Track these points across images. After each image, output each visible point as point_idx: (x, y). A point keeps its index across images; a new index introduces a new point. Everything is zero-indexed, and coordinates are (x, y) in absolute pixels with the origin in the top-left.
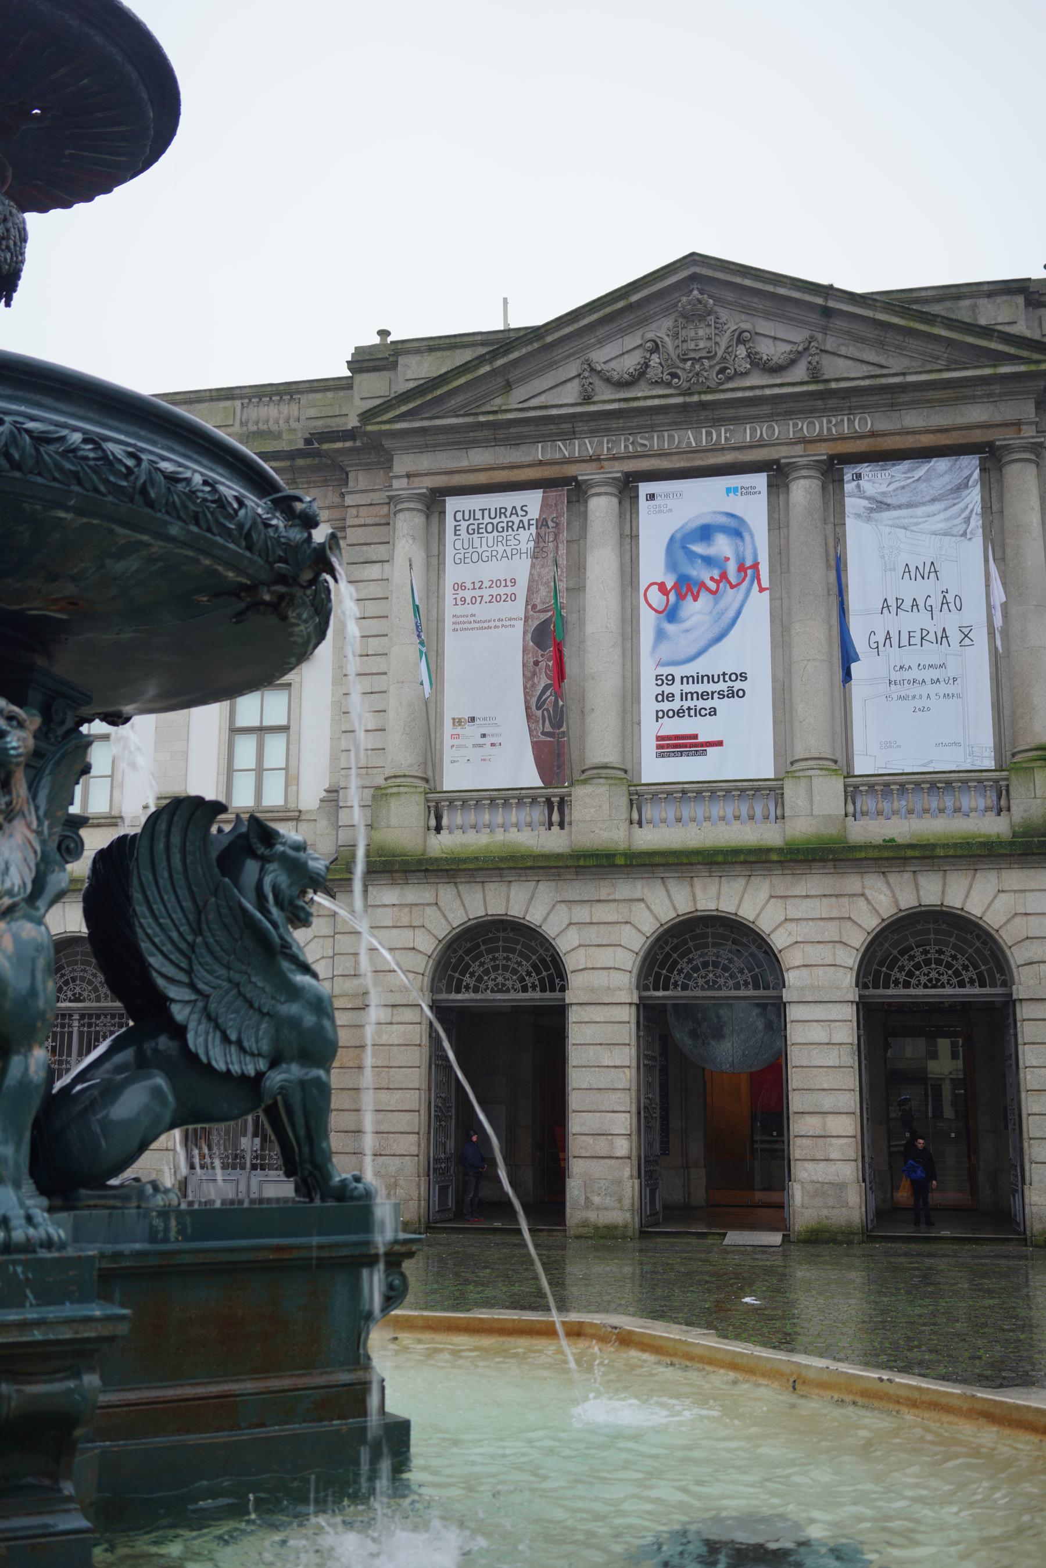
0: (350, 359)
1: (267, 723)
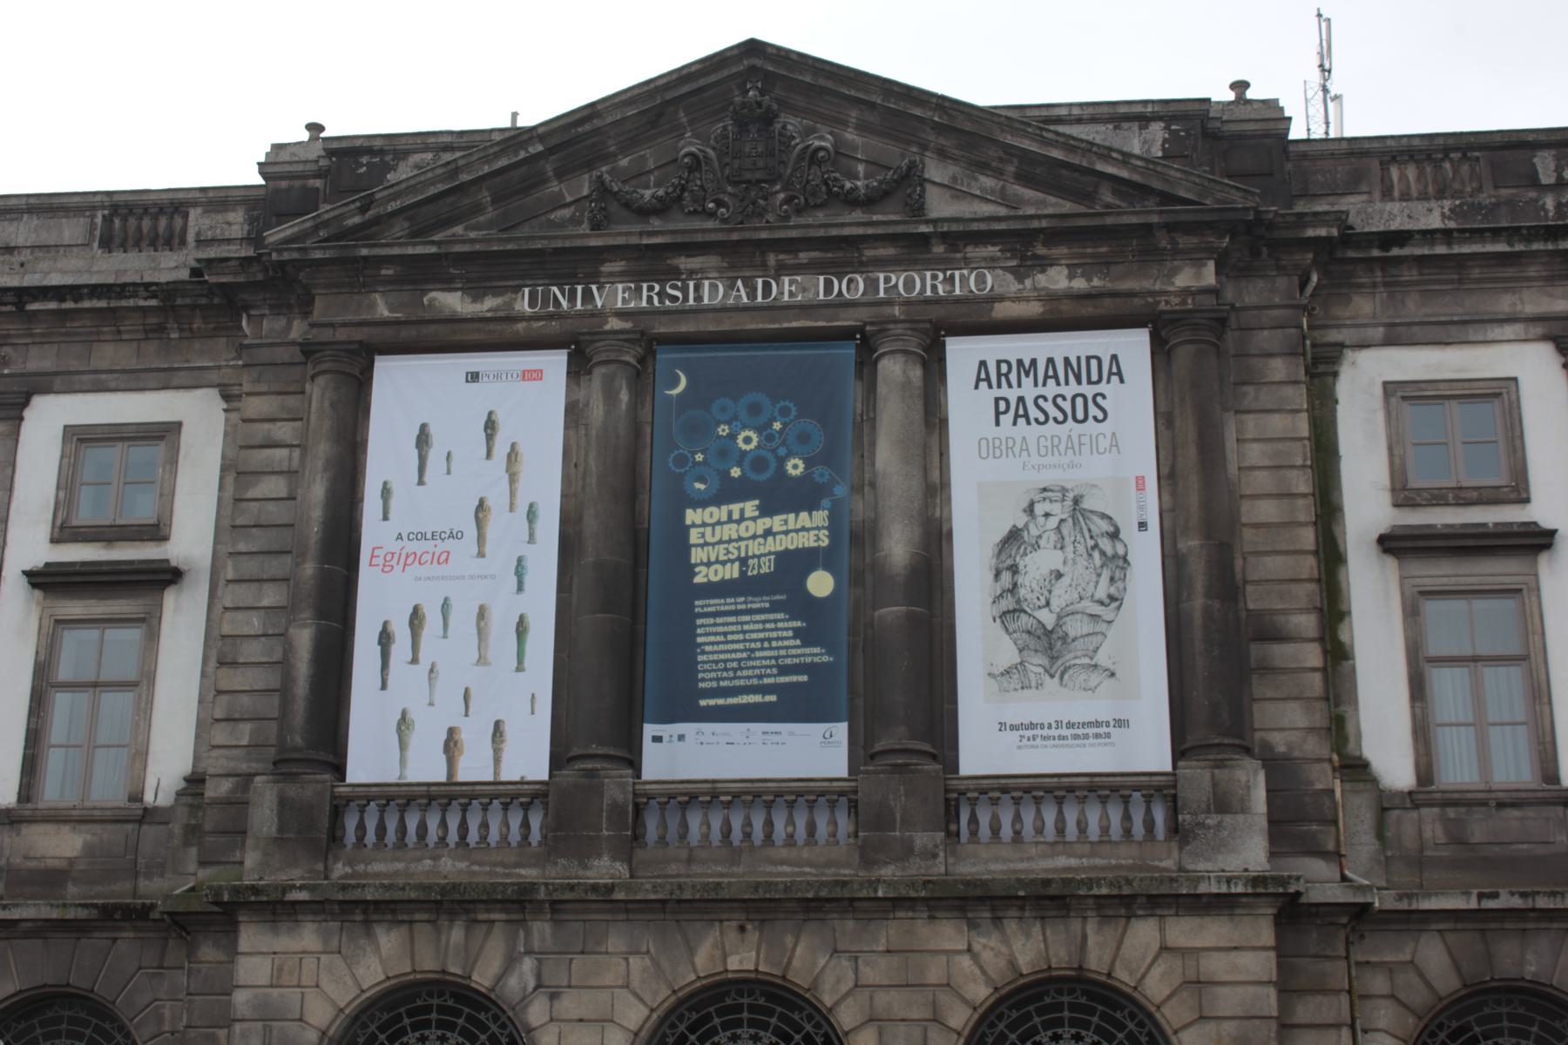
0: (262, 160)
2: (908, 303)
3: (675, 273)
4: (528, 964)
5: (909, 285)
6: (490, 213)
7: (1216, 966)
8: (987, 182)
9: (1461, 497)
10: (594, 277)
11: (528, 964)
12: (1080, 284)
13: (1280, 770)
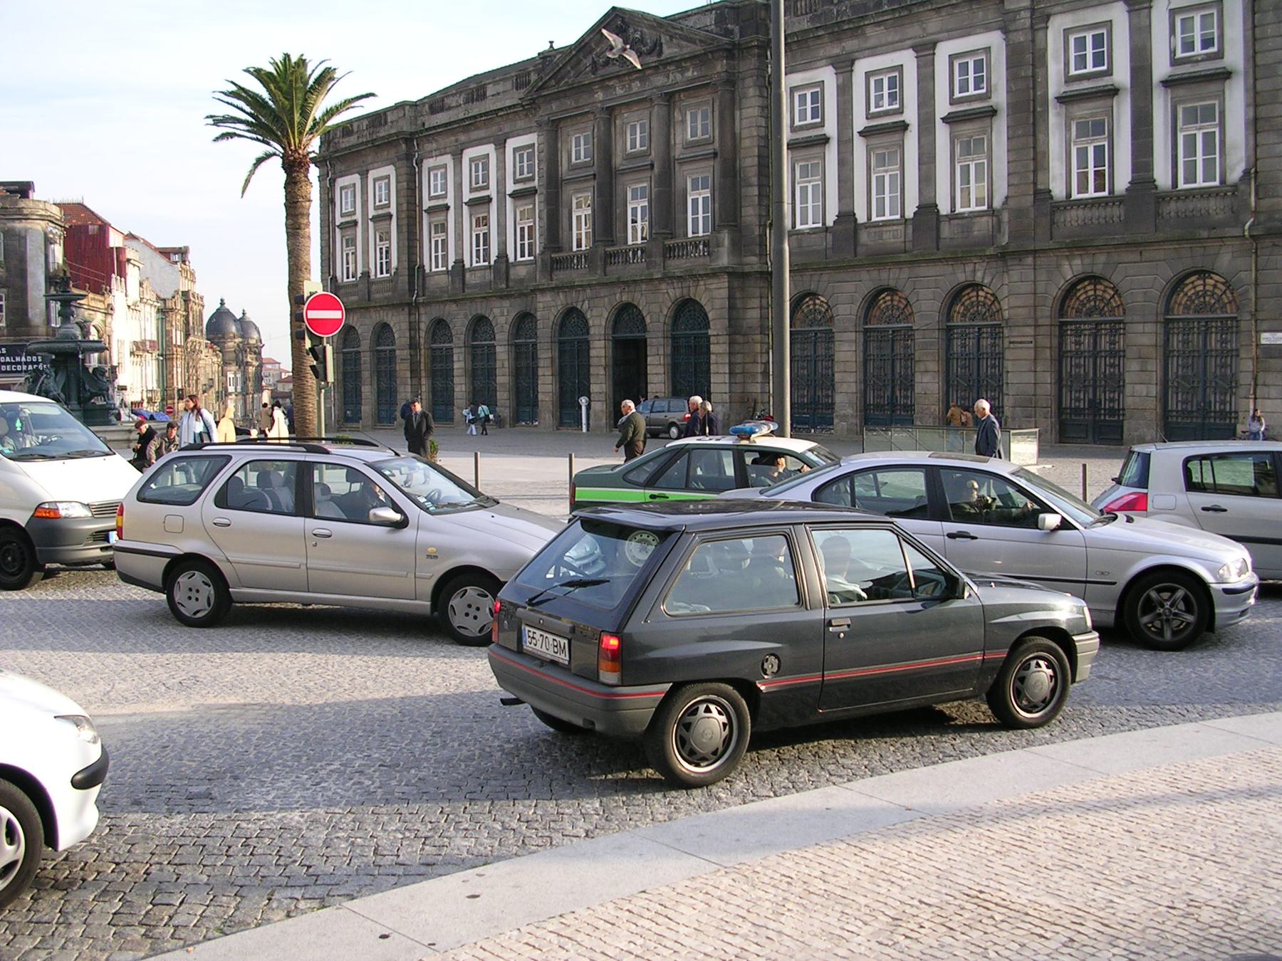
6: (572, 73)
7: (716, 294)
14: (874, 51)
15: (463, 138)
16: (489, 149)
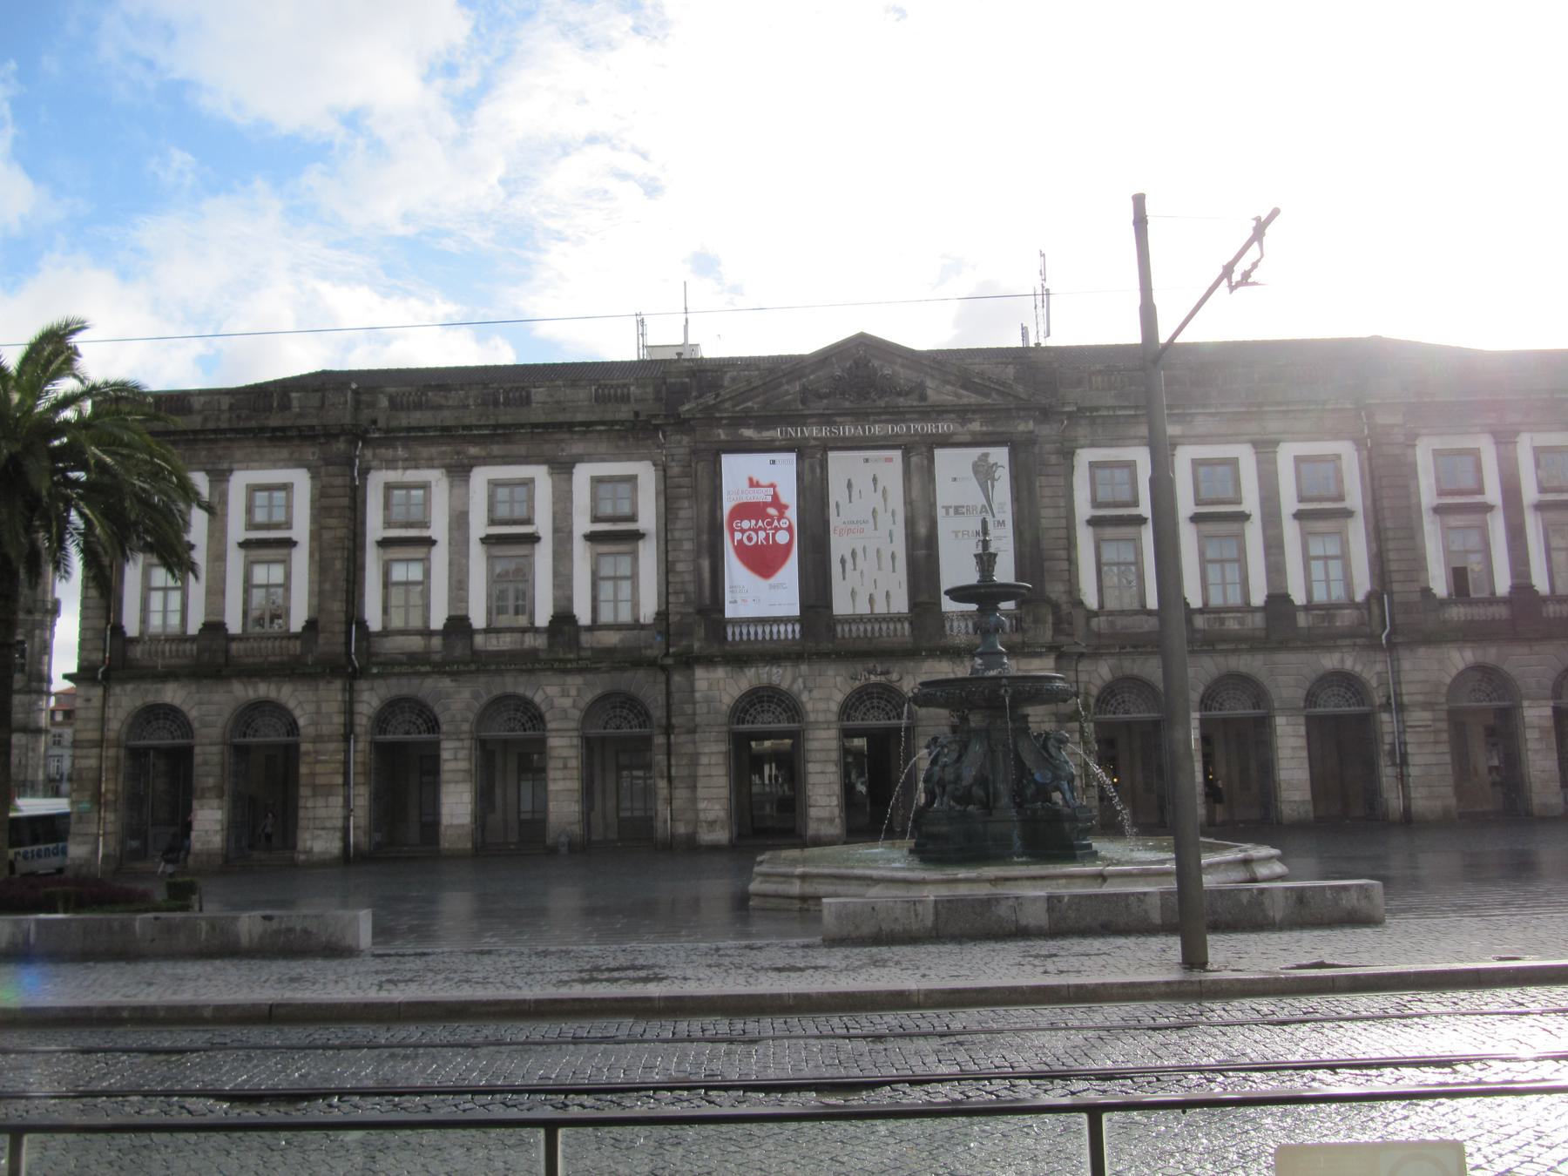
1: (618, 574)
2: (923, 436)
3: (835, 423)
4: (800, 681)
5: (922, 429)
8: (949, 388)
9: (1116, 505)
10: (804, 424)
11: (800, 681)
12: (984, 429)
13: (1056, 607)
14: (1202, 439)
15: (474, 451)
16: (540, 474)
